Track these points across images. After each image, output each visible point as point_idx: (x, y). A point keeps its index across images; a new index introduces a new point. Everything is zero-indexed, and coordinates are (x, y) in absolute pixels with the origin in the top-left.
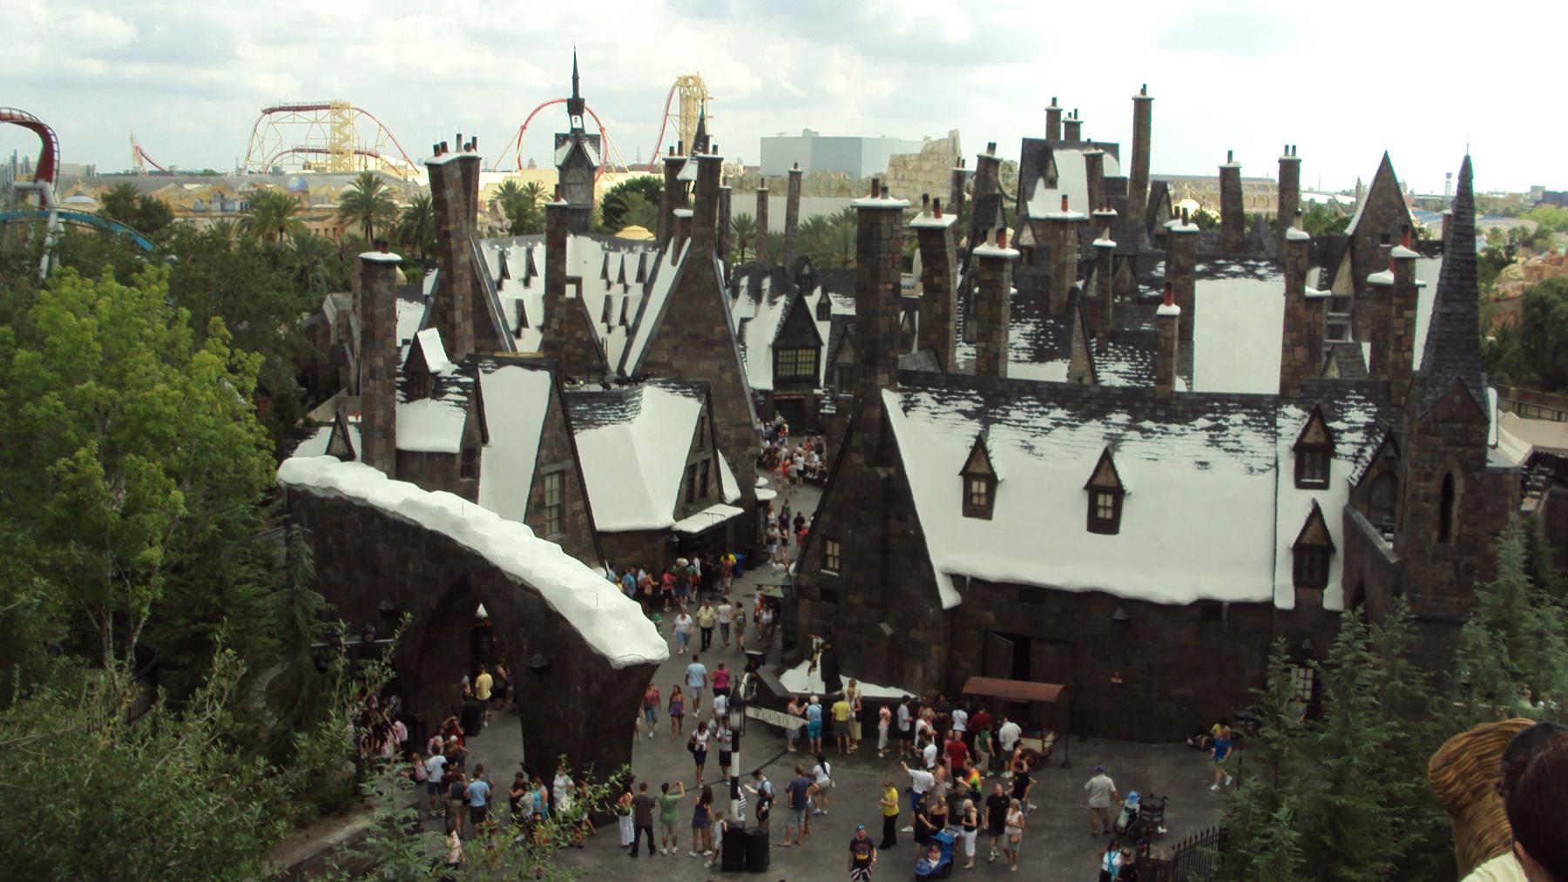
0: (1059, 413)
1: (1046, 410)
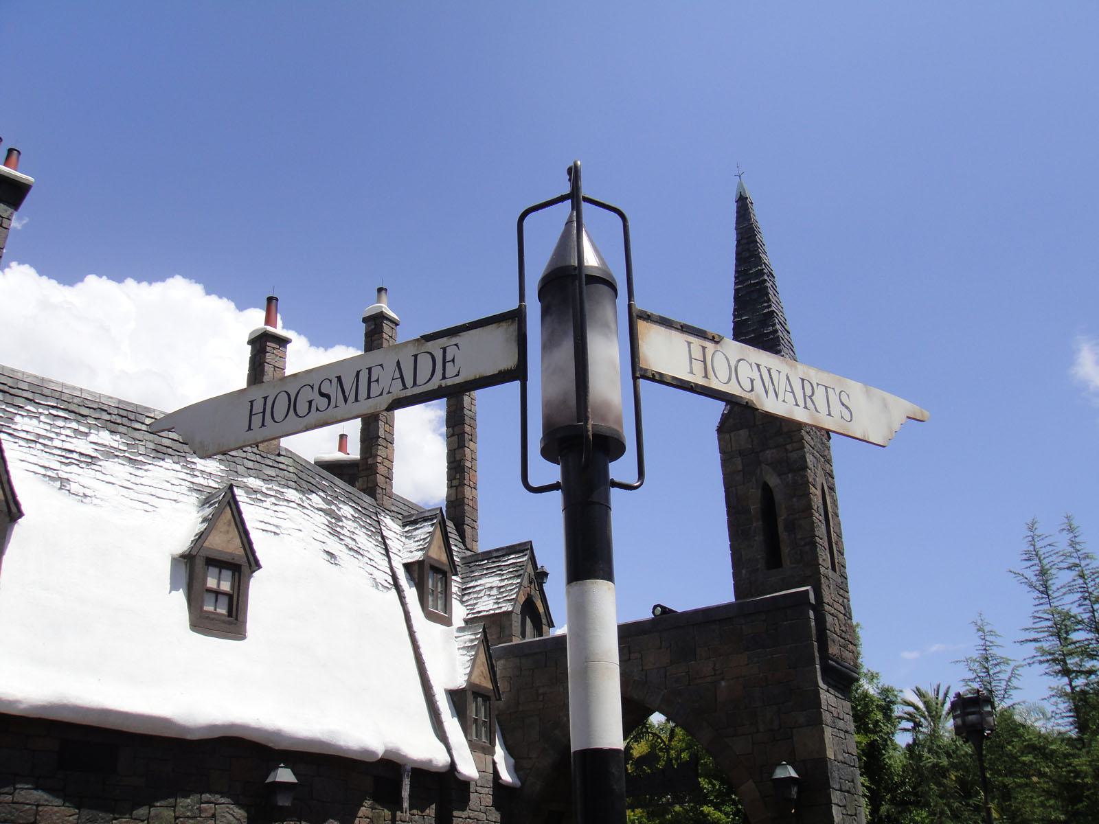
0: (105, 437)
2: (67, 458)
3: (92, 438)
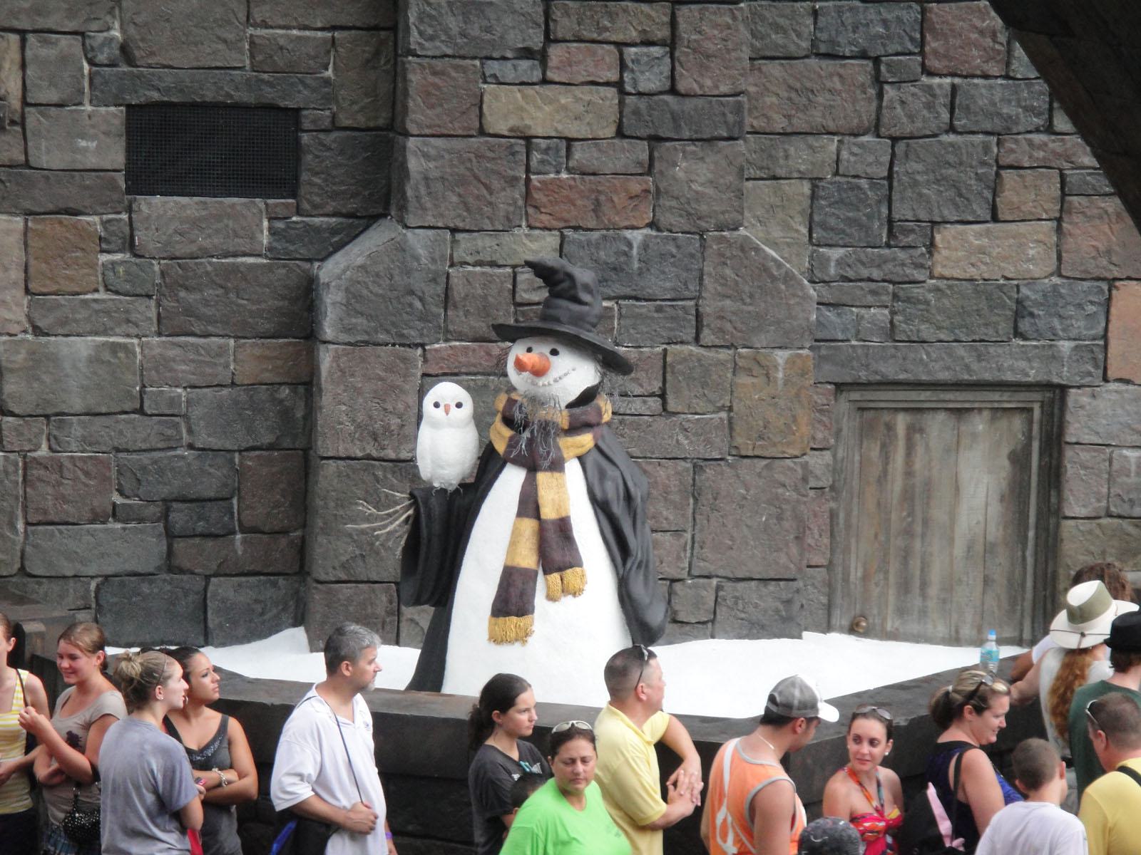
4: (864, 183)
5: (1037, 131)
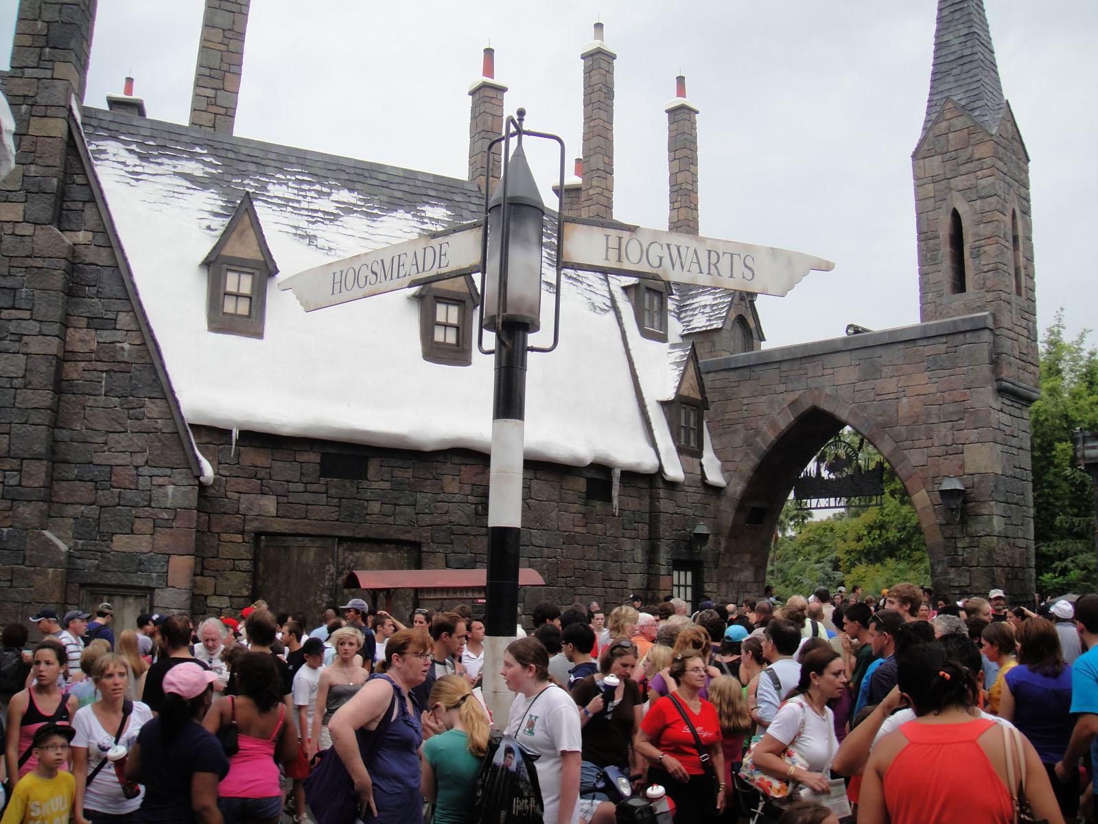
0: (345, 196)
1: (325, 190)
2: (313, 217)
3: (335, 196)
4: (91, 520)
5: (146, 506)
